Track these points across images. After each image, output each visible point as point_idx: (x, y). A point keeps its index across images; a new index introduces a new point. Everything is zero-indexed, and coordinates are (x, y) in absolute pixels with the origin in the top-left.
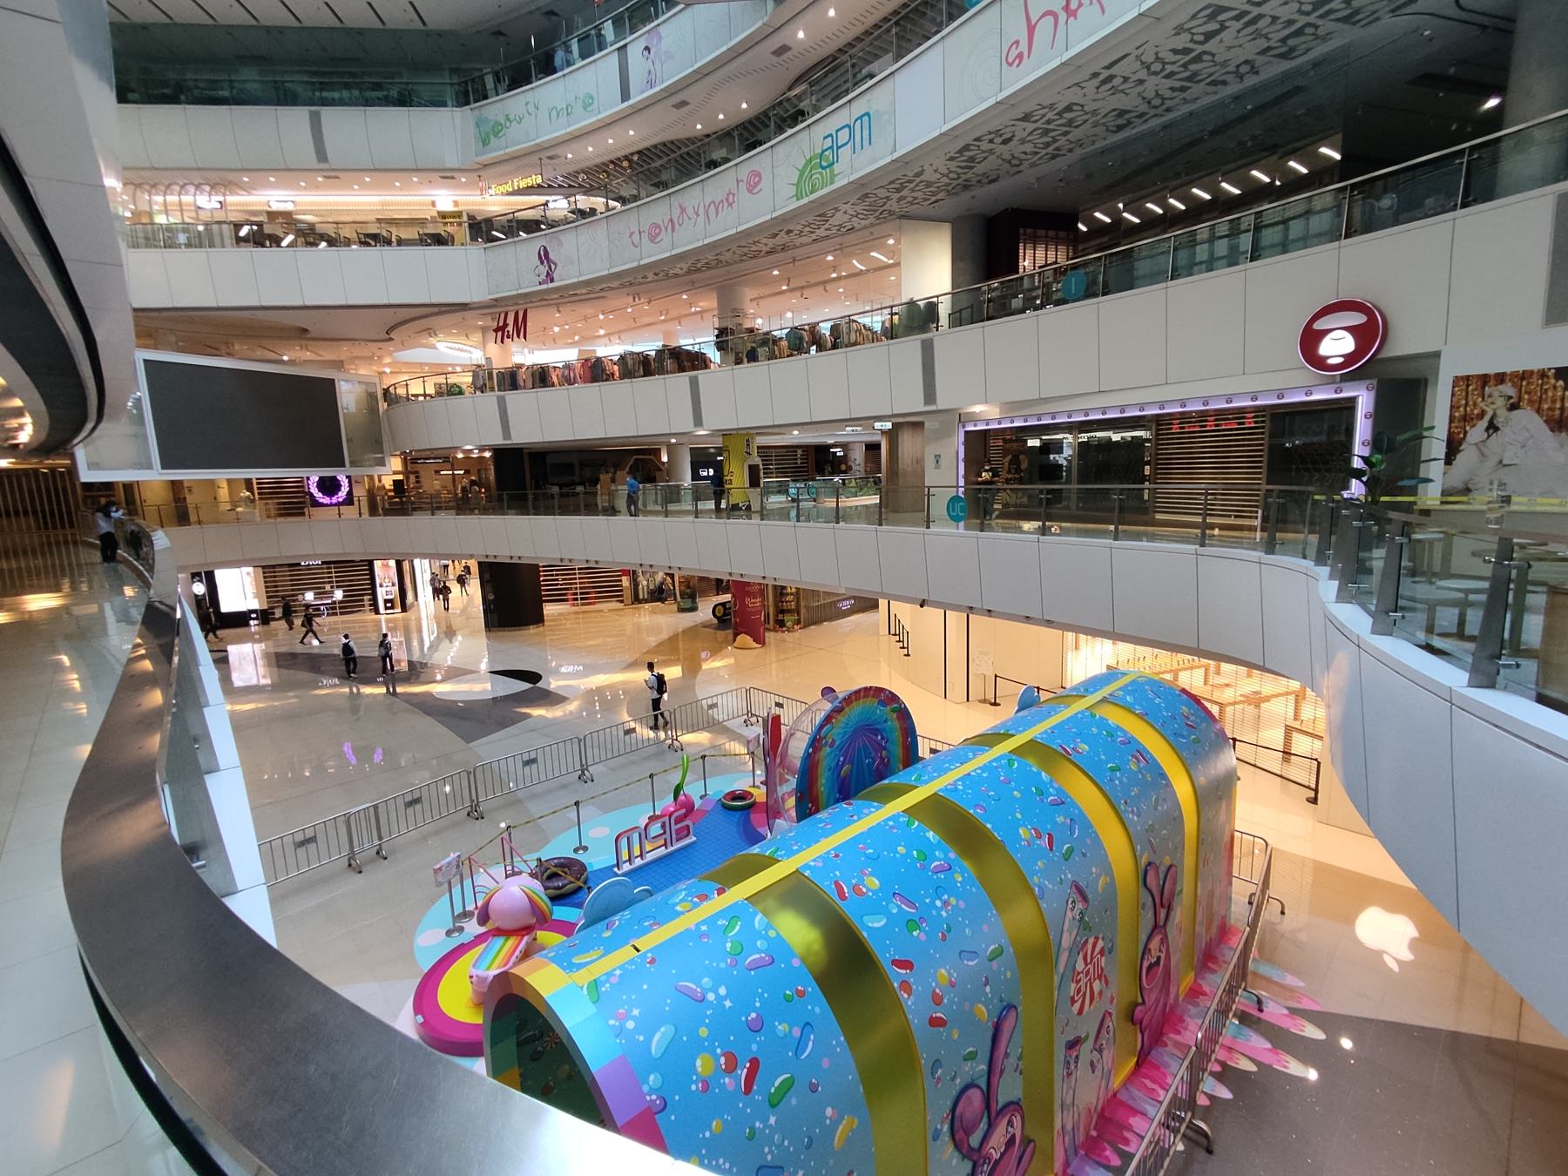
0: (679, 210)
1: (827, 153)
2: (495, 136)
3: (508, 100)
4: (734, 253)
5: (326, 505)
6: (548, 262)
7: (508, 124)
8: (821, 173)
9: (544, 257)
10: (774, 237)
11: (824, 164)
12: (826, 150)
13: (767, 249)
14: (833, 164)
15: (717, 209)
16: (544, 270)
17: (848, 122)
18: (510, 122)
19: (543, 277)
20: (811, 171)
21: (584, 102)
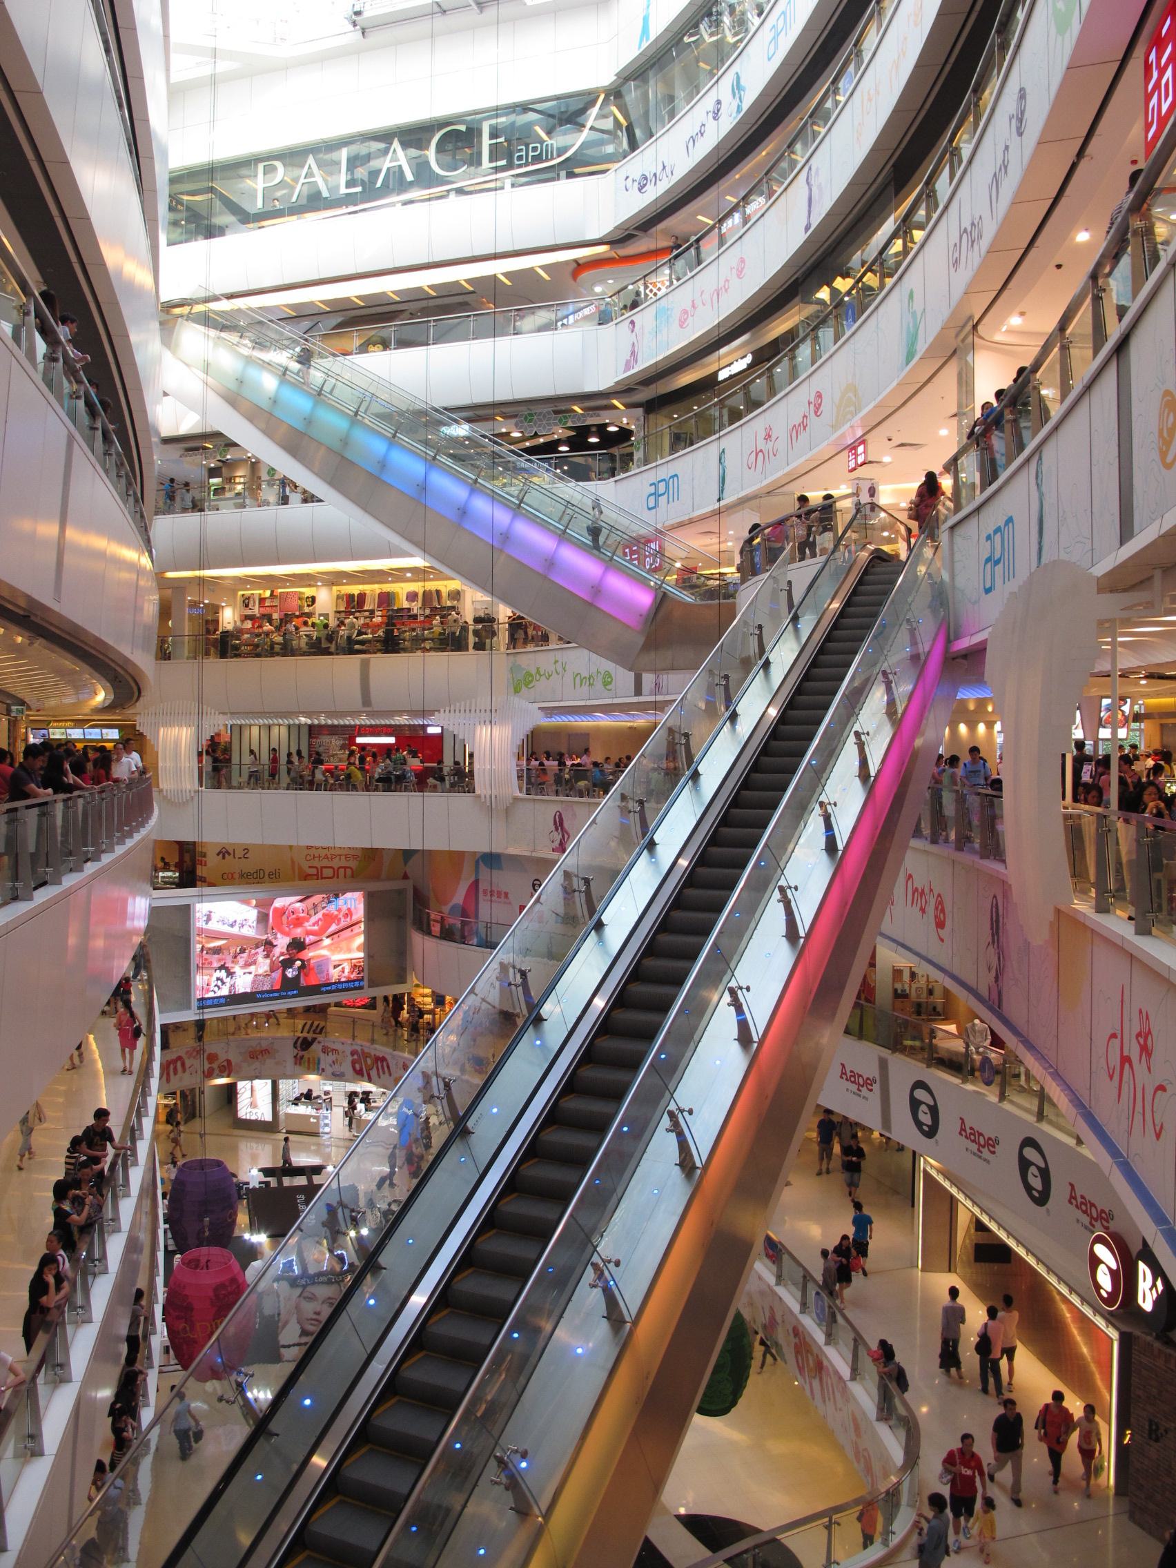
2: (526, 686)
3: (540, 654)
7: (538, 677)
9: (559, 823)
18: (541, 675)
19: (557, 844)
21: (604, 678)
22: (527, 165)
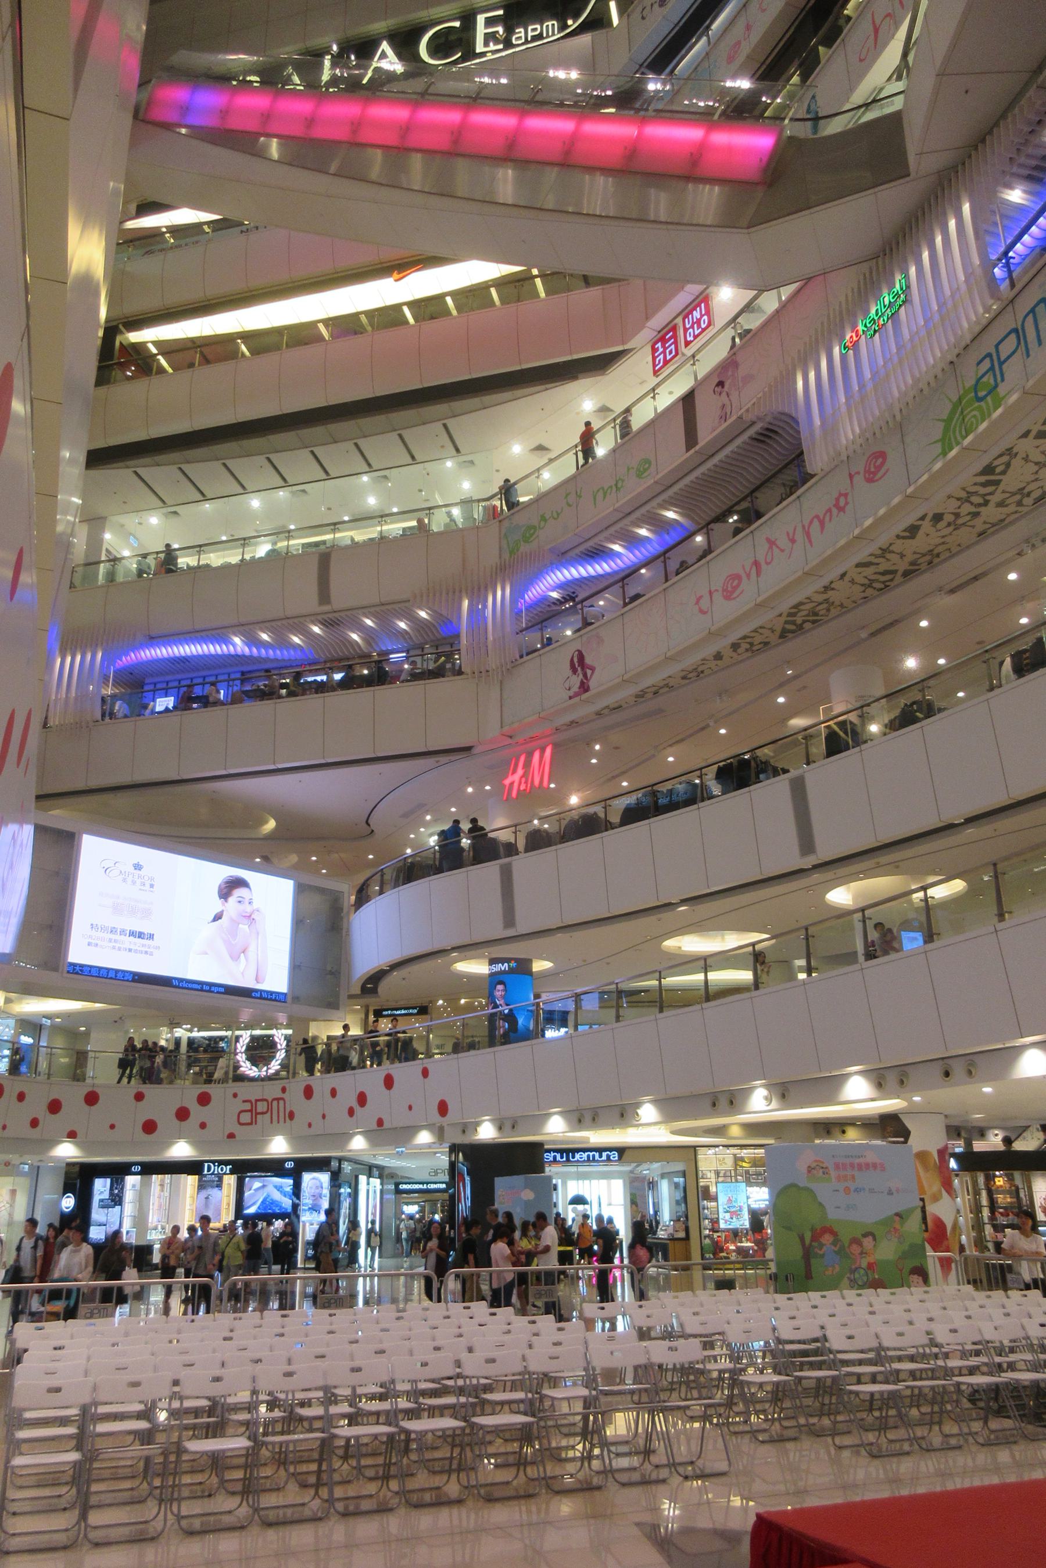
0: (767, 545)
1: (985, 379)
2: (525, 541)
4: (853, 581)
5: (252, 1079)
6: (583, 669)
7: (542, 523)
8: (980, 408)
10: (913, 537)
11: (981, 394)
12: (983, 376)
13: (902, 566)
14: (996, 386)
15: (822, 523)
16: (576, 681)
17: (1014, 326)
18: (546, 521)
19: (576, 688)
20: (962, 412)
22: (527, 42)
